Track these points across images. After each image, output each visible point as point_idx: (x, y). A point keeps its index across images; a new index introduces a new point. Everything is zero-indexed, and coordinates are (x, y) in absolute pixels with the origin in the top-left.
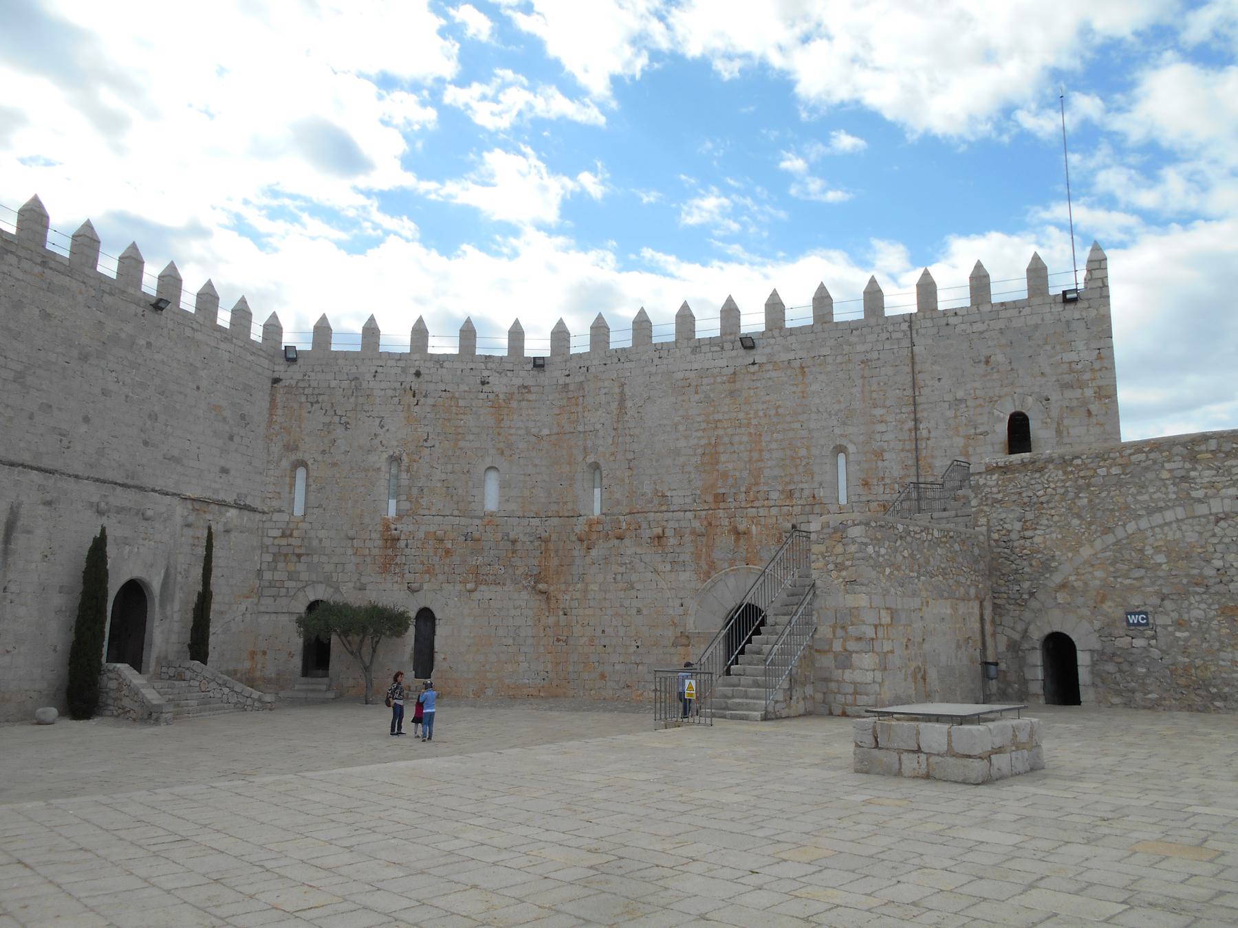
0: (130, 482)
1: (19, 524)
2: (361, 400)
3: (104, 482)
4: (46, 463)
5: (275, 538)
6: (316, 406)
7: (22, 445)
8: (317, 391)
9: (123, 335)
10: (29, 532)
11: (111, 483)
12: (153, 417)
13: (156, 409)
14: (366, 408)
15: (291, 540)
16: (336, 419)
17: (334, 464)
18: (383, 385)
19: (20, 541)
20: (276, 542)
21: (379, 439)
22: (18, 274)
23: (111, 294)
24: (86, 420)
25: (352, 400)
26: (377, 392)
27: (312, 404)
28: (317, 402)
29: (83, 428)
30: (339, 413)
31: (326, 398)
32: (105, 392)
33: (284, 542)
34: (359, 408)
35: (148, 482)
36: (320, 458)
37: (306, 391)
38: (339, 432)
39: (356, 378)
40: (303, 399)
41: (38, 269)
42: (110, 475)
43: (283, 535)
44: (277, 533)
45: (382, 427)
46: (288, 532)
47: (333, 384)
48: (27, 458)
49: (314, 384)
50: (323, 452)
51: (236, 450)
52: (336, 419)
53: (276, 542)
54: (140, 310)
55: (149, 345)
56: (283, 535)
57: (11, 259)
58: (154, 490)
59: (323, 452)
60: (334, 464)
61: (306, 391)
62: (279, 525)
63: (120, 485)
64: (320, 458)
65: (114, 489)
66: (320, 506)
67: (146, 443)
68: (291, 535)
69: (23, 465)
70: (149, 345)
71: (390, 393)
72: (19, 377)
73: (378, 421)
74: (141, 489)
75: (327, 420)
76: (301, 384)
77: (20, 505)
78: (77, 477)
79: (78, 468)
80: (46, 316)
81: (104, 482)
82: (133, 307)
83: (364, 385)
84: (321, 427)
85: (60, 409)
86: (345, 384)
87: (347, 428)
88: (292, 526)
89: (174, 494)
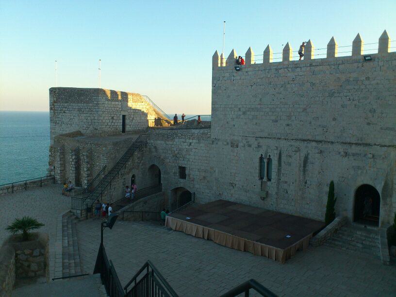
0: (360, 142)
1: (309, 161)
3: (345, 143)
4: (318, 138)
7: (307, 133)
9: (351, 79)
10: (313, 164)
11: (350, 143)
12: (373, 111)
13: (374, 107)
19: (309, 167)
22: (301, 74)
23: (343, 63)
24: (334, 119)
29: (334, 123)
32: (343, 106)
35: (369, 141)
42: (348, 140)
48: (310, 138)
54: (360, 65)
55: (368, 78)
57: (299, 69)
58: (375, 144)
63: (356, 144)
65: (351, 146)
67: (369, 124)
69: (308, 140)
70: (368, 78)
72: (305, 110)
77: (308, 154)
78: (332, 143)
79: (332, 139)
80: (313, 84)
81: (345, 143)
82: (356, 65)
89: (389, 146)
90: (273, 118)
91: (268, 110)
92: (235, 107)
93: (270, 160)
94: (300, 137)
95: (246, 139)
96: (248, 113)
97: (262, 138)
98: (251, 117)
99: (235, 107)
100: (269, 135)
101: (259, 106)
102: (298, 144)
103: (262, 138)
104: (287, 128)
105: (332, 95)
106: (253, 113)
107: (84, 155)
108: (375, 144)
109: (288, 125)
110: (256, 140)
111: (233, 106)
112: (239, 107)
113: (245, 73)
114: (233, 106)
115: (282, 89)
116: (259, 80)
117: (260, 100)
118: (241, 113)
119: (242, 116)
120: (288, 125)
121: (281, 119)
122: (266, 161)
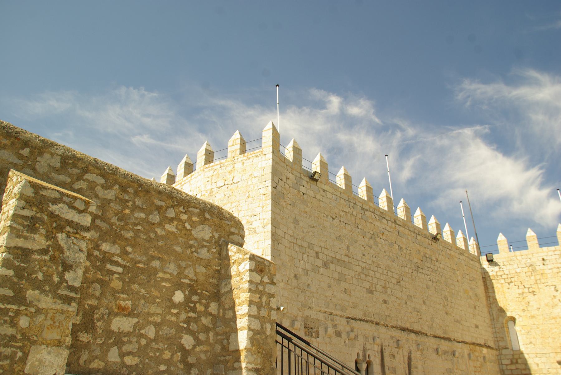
2: (538, 277)
5: (507, 365)
6: (511, 284)
8: (509, 276)
14: (543, 281)
15: (518, 366)
16: (526, 290)
17: (533, 317)
18: (550, 267)
20: (509, 367)
21: (557, 298)
25: (533, 278)
26: (547, 271)
27: (509, 283)
28: (511, 282)
29: (424, 307)
30: (526, 286)
31: (516, 279)
32: (428, 287)
33: (513, 367)
34: (538, 281)
35: (452, 335)
36: (522, 314)
37: (503, 277)
38: (530, 297)
39: (531, 265)
40: (503, 281)
41: (394, 225)
43: (512, 363)
44: (508, 362)
45: (557, 291)
46: (514, 361)
47: (518, 270)
49: (506, 272)
50: (523, 310)
51: (478, 315)
52: (526, 290)
53: (509, 367)
56: (512, 363)
59: (523, 310)
60: (533, 317)
61: (503, 277)
62: (508, 357)
64: (522, 314)
66: (531, 343)
67: (447, 313)
68: (517, 363)
71: (556, 270)
73: (553, 288)
74: (449, 339)
75: (520, 291)
76: (499, 273)
83: (538, 268)
84: (517, 296)
85: (414, 297)
86: (526, 269)
87: (534, 295)
88: (516, 357)
90: (367, 285)
91: (359, 269)
92: (309, 247)
93: (369, 364)
94: (399, 324)
95: (332, 320)
96: (332, 266)
97: (356, 319)
98: (336, 276)
99: (309, 247)
100: (365, 315)
101: (346, 259)
102: (398, 334)
103: (356, 319)
104: (384, 306)
105: (417, 268)
106: (339, 269)
107: (60, 224)
108: (454, 340)
109: (385, 302)
110: (348, 322)
111: (305, 244)
112: (317, 249)
113: (321, 190)
114: (305, 244)
115: (372, 242)
116: (342, 214)
117: (348, 248)
118: (319, 263)
119: (322, 270)
120: (385, 302)
121: (376, 291)
122: (364, 366)
